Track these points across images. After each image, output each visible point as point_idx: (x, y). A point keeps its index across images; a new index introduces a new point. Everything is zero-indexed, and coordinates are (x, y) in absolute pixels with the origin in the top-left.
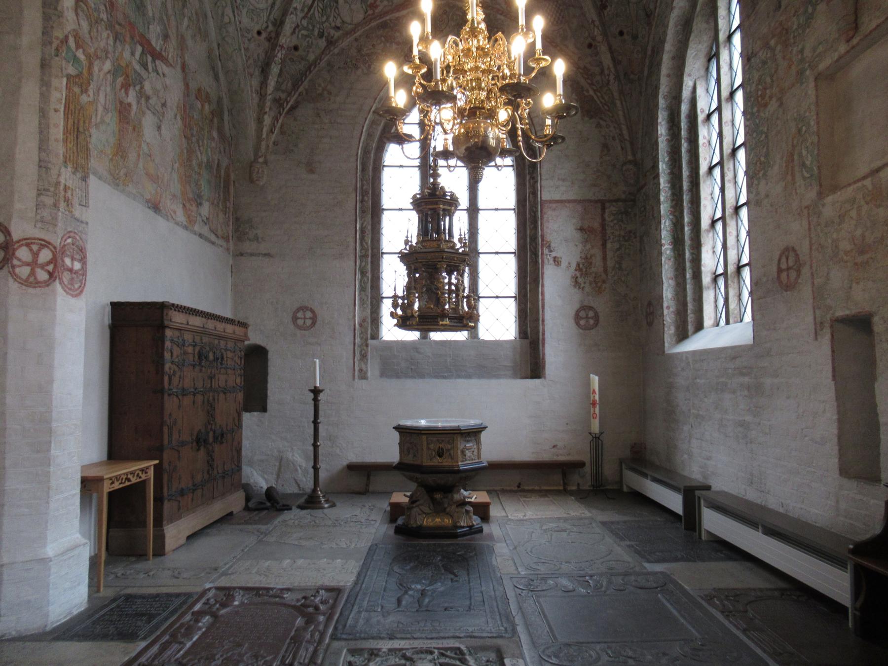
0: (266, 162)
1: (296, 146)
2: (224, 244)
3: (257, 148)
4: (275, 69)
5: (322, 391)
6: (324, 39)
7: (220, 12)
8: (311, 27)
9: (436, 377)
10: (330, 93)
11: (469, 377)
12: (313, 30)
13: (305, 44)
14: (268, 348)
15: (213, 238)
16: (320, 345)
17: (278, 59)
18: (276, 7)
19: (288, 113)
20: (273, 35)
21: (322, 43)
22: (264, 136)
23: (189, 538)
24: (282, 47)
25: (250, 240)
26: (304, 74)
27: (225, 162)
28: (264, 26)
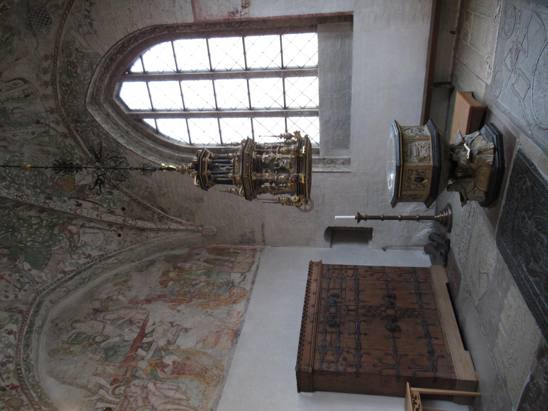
0: (202, 226)
1: (187, 208)
2: (258, 254)
3: (193, 231)
4: (140, 223)
5: (359, 214)
6: (112, 191)
7: (112, 266)
8: (108, 201)
9: (349, 105)
10: (147, 187)
11: (350, 78)
12: (109, 199)
13: (119, 203)
14: (327, 227)
15: (254, 268)
16: (324, 195)
17: (133, 223)
18: (100, 226)
19: (167, 213)
20: (118, 226)
21: (116, 192)
22: (184, 227)
23: (466, 348)
24: (124, 221)
25: (253, 236)
26: (139, 204)
27: (205, 254)
28: (113, 232)
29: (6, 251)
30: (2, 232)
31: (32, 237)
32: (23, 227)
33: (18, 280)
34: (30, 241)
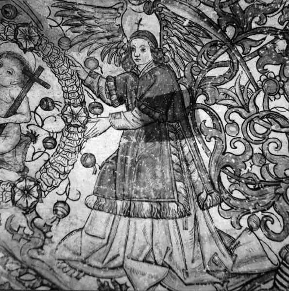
29: (145, 58)
30: (211, 13)
31: (235, 117)
32: (260, 66)
33: (33, 137)
34: (214, 116)
